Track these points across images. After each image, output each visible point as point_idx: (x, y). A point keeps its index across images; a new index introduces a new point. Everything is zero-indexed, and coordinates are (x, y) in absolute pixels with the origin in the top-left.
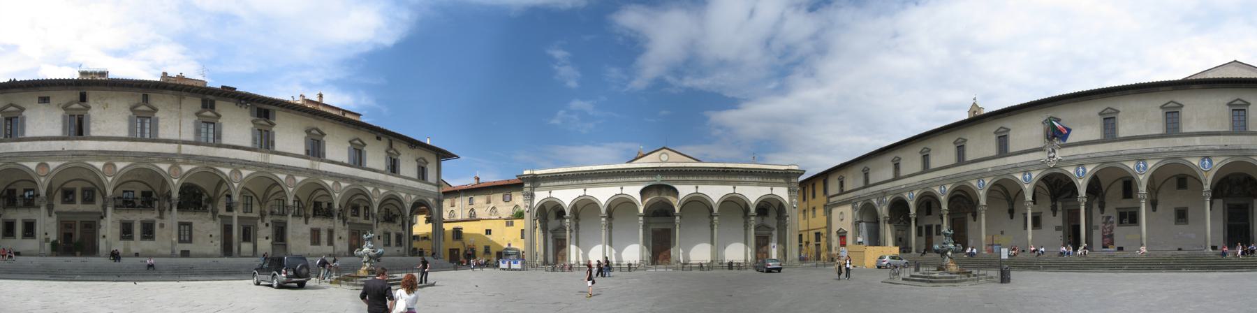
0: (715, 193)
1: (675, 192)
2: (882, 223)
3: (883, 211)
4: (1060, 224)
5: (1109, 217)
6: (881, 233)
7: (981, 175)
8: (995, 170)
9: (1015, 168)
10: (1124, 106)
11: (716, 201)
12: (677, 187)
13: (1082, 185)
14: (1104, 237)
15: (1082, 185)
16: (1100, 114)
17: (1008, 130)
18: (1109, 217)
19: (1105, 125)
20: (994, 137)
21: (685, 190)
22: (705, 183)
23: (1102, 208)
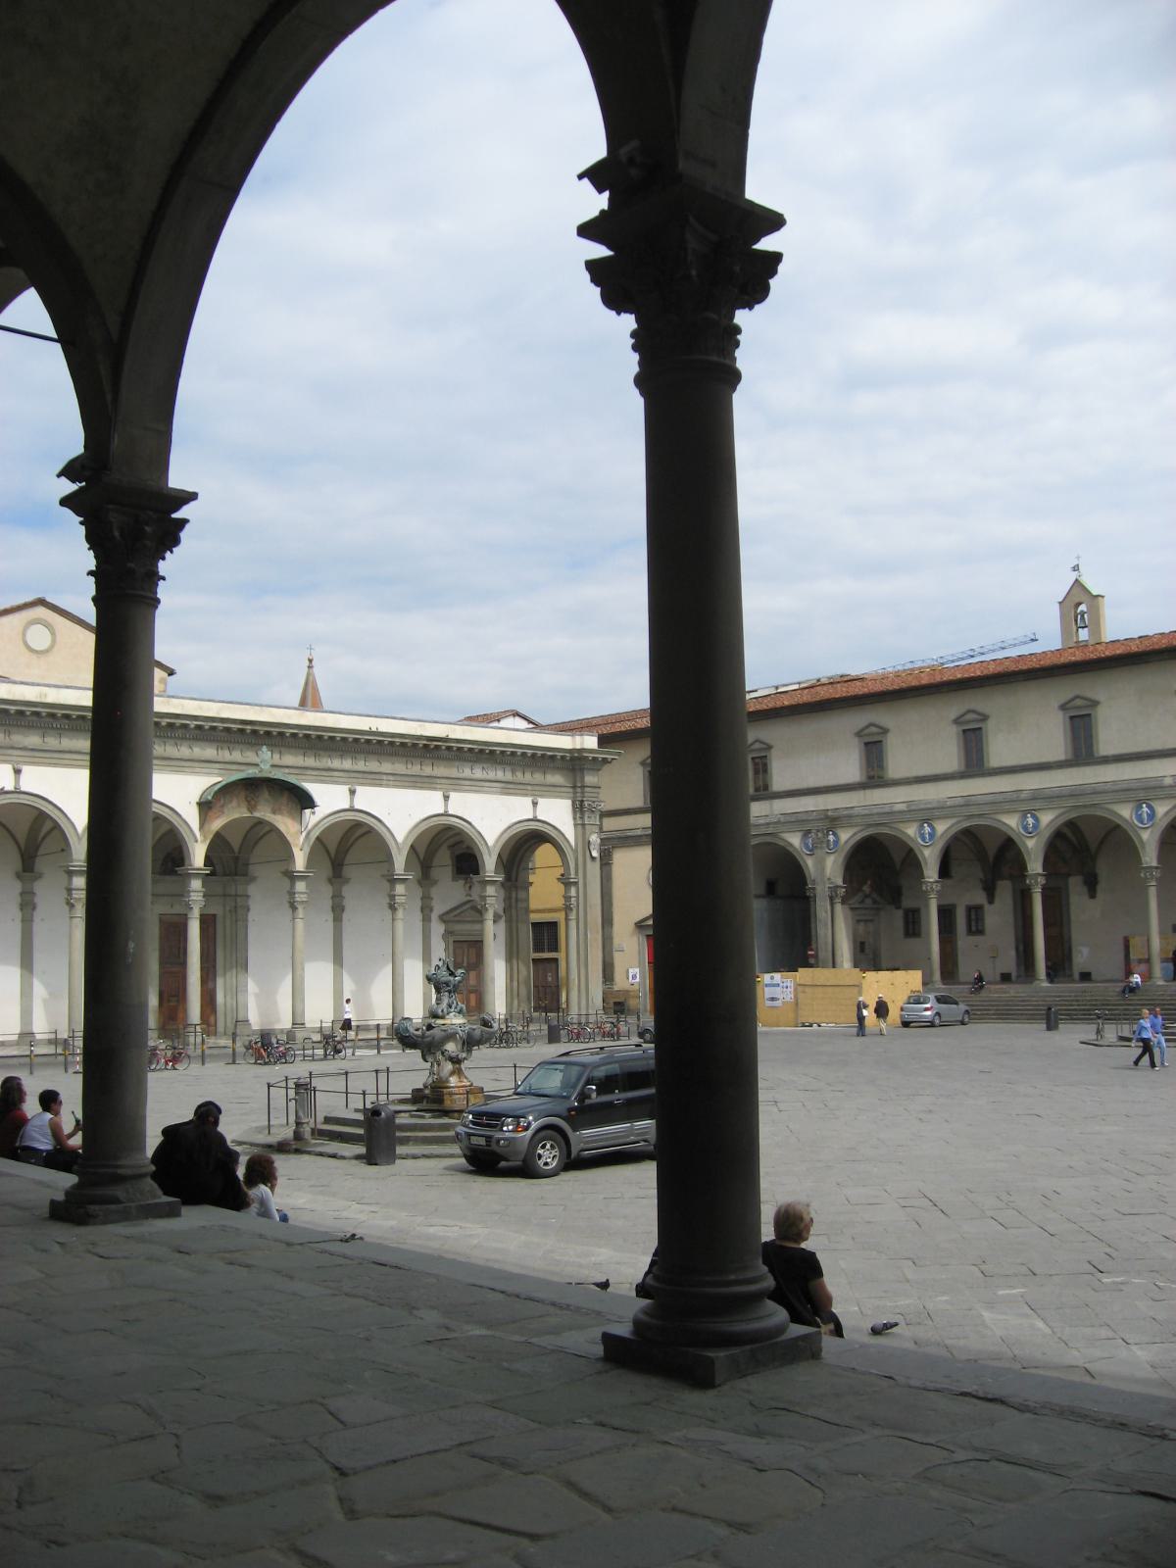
0: (401, 810)
1: (306, 801)
2: (822, 909)
3: (826, 869)
6: (822, 932)
12: (313, 788)
21: (330, 799)
22: (374, 779)
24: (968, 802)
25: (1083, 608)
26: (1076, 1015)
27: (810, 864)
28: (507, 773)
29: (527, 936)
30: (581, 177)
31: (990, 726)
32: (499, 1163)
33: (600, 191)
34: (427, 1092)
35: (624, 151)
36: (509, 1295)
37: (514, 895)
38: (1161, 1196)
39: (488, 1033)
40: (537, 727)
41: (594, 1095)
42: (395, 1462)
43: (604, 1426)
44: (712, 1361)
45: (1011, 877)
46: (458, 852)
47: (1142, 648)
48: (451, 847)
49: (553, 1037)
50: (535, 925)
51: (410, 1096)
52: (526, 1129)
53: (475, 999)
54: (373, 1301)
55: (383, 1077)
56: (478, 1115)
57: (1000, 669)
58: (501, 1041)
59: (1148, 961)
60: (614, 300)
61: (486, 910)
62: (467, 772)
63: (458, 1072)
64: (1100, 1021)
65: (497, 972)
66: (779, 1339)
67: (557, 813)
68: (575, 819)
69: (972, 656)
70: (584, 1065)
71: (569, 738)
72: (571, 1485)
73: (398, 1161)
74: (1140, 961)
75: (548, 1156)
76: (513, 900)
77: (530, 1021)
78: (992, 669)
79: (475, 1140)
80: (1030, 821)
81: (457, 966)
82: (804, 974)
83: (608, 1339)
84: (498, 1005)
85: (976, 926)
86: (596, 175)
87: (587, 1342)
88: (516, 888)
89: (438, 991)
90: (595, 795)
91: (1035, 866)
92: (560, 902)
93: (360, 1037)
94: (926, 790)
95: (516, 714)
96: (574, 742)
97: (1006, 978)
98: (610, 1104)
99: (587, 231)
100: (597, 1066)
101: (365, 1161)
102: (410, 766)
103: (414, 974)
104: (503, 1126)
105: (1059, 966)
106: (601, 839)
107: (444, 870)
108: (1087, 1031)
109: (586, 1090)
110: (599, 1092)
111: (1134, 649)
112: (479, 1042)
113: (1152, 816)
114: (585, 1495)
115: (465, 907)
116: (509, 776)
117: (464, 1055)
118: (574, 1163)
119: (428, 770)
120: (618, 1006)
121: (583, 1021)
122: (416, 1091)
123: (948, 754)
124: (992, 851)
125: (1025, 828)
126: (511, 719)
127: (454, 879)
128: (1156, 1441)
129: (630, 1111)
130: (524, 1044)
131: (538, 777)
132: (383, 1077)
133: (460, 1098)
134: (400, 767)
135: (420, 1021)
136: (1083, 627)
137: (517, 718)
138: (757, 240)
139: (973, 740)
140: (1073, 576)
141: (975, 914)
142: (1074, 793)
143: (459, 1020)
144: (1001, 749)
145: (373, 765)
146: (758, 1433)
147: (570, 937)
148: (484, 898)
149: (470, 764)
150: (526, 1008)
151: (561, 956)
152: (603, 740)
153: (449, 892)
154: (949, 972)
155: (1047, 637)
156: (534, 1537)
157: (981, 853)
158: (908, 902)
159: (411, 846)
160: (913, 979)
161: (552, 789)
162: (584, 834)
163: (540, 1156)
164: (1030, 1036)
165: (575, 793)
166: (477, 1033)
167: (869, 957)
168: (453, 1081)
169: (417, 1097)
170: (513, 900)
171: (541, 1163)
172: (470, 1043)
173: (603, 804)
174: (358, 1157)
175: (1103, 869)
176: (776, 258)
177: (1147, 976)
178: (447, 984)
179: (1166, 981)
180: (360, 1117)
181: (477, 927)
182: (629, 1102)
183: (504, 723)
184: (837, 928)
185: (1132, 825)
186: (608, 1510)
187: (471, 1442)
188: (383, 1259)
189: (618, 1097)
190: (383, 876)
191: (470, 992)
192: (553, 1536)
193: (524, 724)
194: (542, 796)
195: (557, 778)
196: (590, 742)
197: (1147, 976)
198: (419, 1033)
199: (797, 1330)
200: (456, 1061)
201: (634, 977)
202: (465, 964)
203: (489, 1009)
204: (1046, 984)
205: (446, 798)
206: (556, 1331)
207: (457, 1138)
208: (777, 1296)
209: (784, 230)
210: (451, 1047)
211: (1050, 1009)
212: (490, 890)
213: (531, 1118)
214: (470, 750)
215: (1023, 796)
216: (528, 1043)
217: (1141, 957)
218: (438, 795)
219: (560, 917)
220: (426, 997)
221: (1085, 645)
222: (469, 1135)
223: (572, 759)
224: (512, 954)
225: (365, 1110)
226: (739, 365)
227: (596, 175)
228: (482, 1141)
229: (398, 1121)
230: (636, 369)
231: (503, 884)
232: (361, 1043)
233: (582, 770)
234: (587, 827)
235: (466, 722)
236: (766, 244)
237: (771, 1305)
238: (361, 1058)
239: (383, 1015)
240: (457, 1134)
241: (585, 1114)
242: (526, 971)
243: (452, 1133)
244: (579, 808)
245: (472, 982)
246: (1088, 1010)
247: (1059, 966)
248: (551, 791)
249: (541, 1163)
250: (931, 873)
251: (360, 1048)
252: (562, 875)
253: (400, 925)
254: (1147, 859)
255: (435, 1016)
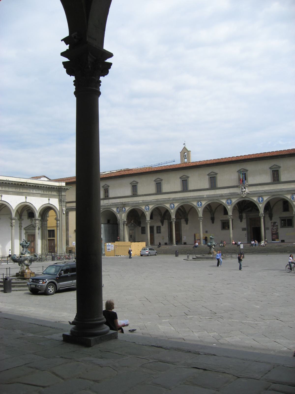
2: (121, 227)
3: (122, 217)
4: (245, 226)
5: (275, 223)
6: (121, 233)
7: (199, 199)
8: (208, 197)
9: (222, 196)
10: (282, 164)
11: (14, 208)
13: (261, 207)
14: (273, 234)
15: (261, 207)
16: (270, 168)
17: (216, 174)
18: (275, 223)
19: (273, 174)
20: (207, 177)
23: (271, 217)
24: (157, 201)
25: (186, 154)
26: (183, 253)
27: (118, 215)
28: (42, 192)
29: (47, 233)
30: (62, 40)
31: (163, 182)
32: (39, 291)
33: (67, 44)
34: (20, 274)
35: (73, 35)
36: (39, 325)
37: (43, 223)
38: (201, 296)
39: (36, 258)
40: (50, 180)
41: (63, 274)
42: (8, 369)
43: (62, 358)
44: (90, 340)
45: (168, 219)
46: (29, 212)
47: (199, 164)
48: (27, 210)
49: (53, 259)
50: (49, 231)
51: (15, 275)
52: (45, 283)
53: (33, 250)
54: (4, 328)
55: (8, 270)
56: (33, 279)
57: (166, 168)
58: (40, 260)
59: (200, 240)
60: (70, 72)
61: (36, 227)
62: (31, 191)
63: (28, 268)
64: (188, 254)
65: (39, 243)
66: (107, 334)
67: (55, 202)
68: (59, 204)
69: (159, 165)
70: (60, 266)
71: (58, 183)
72: (54, 373)
73: (12, 292)
74: (198, 240)
75: (51, 290)
76: (43, 224)
77: (47, 255)
78: (164, 168)
79: (32, 286)
80: (172, 205)
81: (28, 241)
82: (116, 243)
83: (64, 336)
84: (39, 251)
85: (159, 231)
86: (66, 40)
87: (59, 337)
88: (44, 221)
89: (23, 247)
90: (65, 198)
91: (173, 217)
92: (55, 225)
93: (3, 260)
94: (147, 198)
95: (45, 177)
96: (59, 184)
97: (166, 244)
98: (67, 276)
99: (63, 54)
100: (64, 266)
101: (3, 292)
102: (17, 189)
103: (17, 243)
104: (39, 282)
105: (179, 241)
106: (66, 209)
107: (25, 217)
108: (185, 257)
109: (61, 273)
110: (64, 273)
111: (198, 164)
112: (34, 261)
113: (201, 205)
114: (57, 375)
115: (31, 226)
116: (42, 193)
117: (30, 264)
118: (58, 291)
119: (21, 191)
120: (70, 251)
121: (61, 255)
122: (17, 273)
123: (152, 189)
124: (163, 213)
125: (171, 207)
126: (43, 178)
127: (28, 219)
128: (197, 355)
129: (71, 278)
130: (46, 261)
131: (50, 193)
132: (8, 270)
133: (28, 275)
134: (14, 190)
135: (19, 255)
136: (186, 159)
137: (45, 178)
138: (106, 60)
139: (159, 186)
140: (184, 146)
141: (159, 228)
142: (183, 199)
143: (28, 255)
144: (166, 188)
145: (7, 189)
146: (102, 358)
147: (58, 234)
148: (35, 224)
149: (32, 189)
150: (46, 252)
151: (55, 238)
152: (67, 184)
153: (27, 222)
154: (152, 242)
155: (177, 161)
156: (44, 387)
157: (161, 213)
158: (142, 225)
159: (17, 210)
160: (143, 244)
161: (53, 196)
162: (61, 207)
163: (49, 290)
164: (171, 258)
165: (59, 197)
166: (33, 258)
167: (133, 239)
168: (27, 271)
169: (17, 275)
170: (43, 224)
171: (49, 291)
172: (31, 261)
173: (66, 200)
174: (2, 291)
175: (189, 217)
176: (110, 64)
177: (200, 243)
178: (25, 246)
179: (204, 244)
180: (2, 280)
181: (34, 231)
182: (72, 276)
183: (42, 179)
184: (125, 231)
185: (196, 207)
186: (63, 379)
187: (28, 364)
188: (6, 317)
189: (69, 274)
190: (9, 218)
191: (32, 248)
192: (49, 386)
193: (47, 179)
194: (51, 198)
195: (55, 193)
196: (63, 184)
197: (200, 243)
198: (18, 258)
199: (112, 332)
200: (27, 265)
201: (74, 244)
202: (30, 241)
203: (36, 252)
204: (175, 245)
205: (26, 198)
206: (51, 334)
207: (28, 285)
208: (107, 323)
209: (113, 57)
210: (26, 262)
211: (176, 251)
212: (37, 222)
213: (47, 280)
214: (33, 186)
215: (171, 199)
216: (47, 261)
217: (198, 239)
218: (24, 197)
219: (55, 229)
220: (20, 249)
221: (186, 163)
222: (31, 285)
223: (59, 188)
224: (43, 238)
225: (3, 279)
226: (100, 90)
227: (66, 40)
228: (34, 286)
229: (12, 281)
230: (75, 90)
231: (40, 220)
232: (3, 261)
233: (61, 191)
234: (62, 206)
235: (32, 179)
236: (108, 61)
237: (105, 326)
238: (3, 265)
239: (8, 253)
240: (28, 284)
241: (61, 279)
242: (46, 242)
243: (26, 284)
244: (60, 201)
245: (32, 245)
246: (185, 252)
247: (179, 241)
248: (53, 196)
249: (49, 291)
250: (148, 218)
251: (3, 262)
252: (56, 218)
253: (13, 231)
254: (200, 215)
255: (22, 254)
